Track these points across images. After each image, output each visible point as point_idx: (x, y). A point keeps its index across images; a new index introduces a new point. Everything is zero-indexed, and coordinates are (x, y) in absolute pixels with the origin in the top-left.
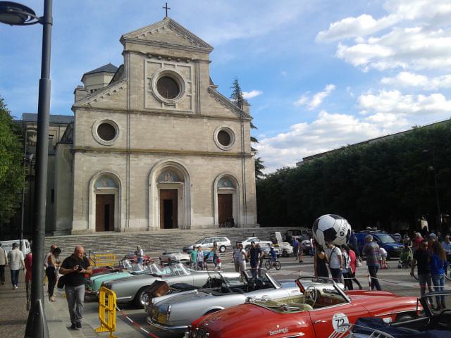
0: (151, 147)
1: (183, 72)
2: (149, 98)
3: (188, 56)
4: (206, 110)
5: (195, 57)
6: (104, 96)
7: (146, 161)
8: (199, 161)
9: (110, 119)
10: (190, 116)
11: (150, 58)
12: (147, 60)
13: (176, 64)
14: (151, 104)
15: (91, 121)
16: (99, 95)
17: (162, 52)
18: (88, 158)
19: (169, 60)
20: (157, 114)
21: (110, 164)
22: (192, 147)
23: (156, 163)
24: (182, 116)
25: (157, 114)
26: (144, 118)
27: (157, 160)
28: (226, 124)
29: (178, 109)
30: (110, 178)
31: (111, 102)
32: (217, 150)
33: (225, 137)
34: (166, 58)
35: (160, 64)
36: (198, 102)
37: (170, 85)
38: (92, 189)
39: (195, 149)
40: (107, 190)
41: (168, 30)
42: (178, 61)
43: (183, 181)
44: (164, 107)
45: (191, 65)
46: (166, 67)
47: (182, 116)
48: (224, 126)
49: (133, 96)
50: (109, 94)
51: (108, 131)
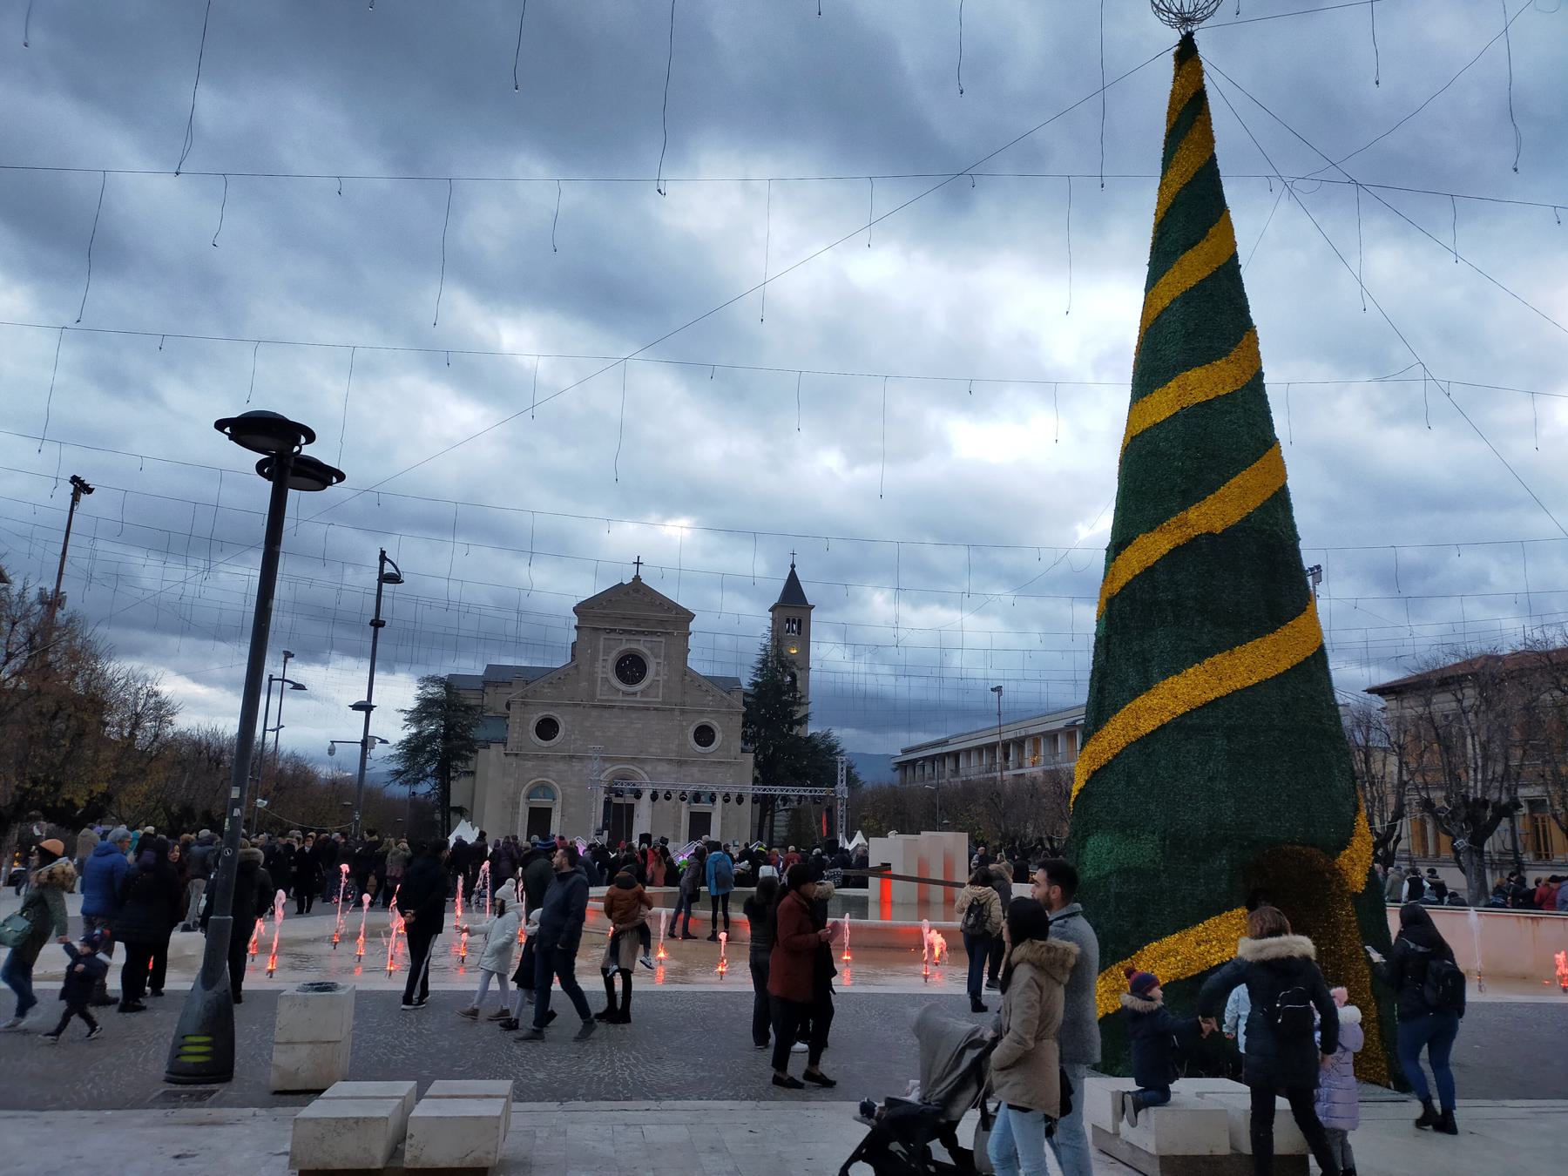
1: (651, 649)
12: (604, 636)
13: (643, 638)
14: (602, 695)
26: (595, 713)
28: (704, 720)
29: (638, 698)
30: (544, 789)
33: (704, 735)
34: (629, 632)
37: (631, 668)
38: (522, 800)
40: (540, 802)
46: (626, 645)
49: (584, 684)
51: (547, 728)
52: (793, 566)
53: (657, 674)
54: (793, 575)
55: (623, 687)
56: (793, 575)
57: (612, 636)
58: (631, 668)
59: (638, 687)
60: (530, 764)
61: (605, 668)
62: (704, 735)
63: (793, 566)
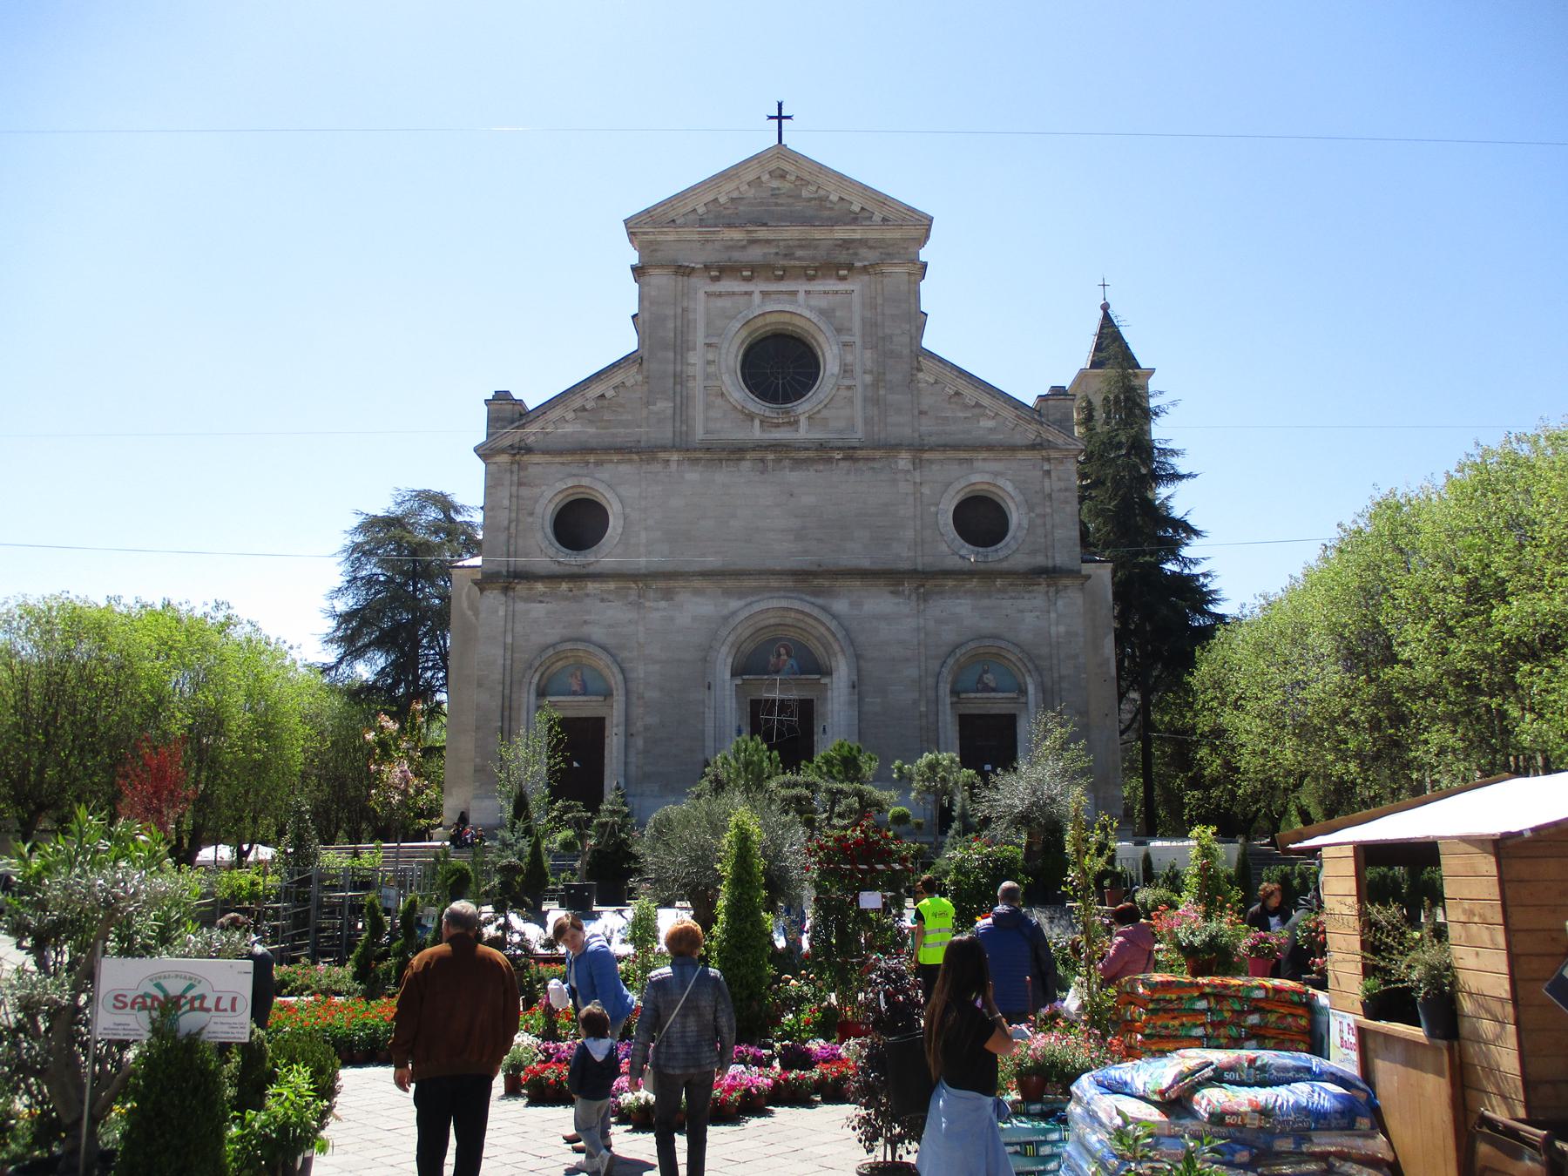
0: (712, 561)
2: (708, 406)
3: (843, 257)
4: (900, 426)
5: (869, 256)
6: (570, 416)
7: (696, 609)
8: (879, 603)
9: (585, 481)
10: (851, 453)
11: (716, 279)
13: (801, 287)
15: (524, 491)
16: (554, 415)
17: (755, 254)
18: (520, 606)
19: (781, 278)
20: (735, 452)
21: (585, 622)
22: (856, 554)
23: (726, 619)
24: (822, 453)
25: (735, 452)
27: (734, 604)
28: (983, 475)
29: (803, 433)
31: (592, 430)
32: (953, 562)
33: (980, 519)
35: (749, 294)
36: (872, 401)
39: (866, 563)
41: (775, 184)
42: (811, 278)
43: (828, 673)
44: (756, 433)
45: (855, 285)
47: (822, 453)
48: (976, 478)
50: (584, 409)
51: (579, 523)
52: (1105, 307)
53: (846, 370)
54: (1107, 318)
55: (756, 406)
56: (1107, 318)
57: (727, 285)
58: (779, 366)
59: (803, 407)
60: (538, 610)
61: (716, 368)
62: (980, 519)
63: (1105, 307)
